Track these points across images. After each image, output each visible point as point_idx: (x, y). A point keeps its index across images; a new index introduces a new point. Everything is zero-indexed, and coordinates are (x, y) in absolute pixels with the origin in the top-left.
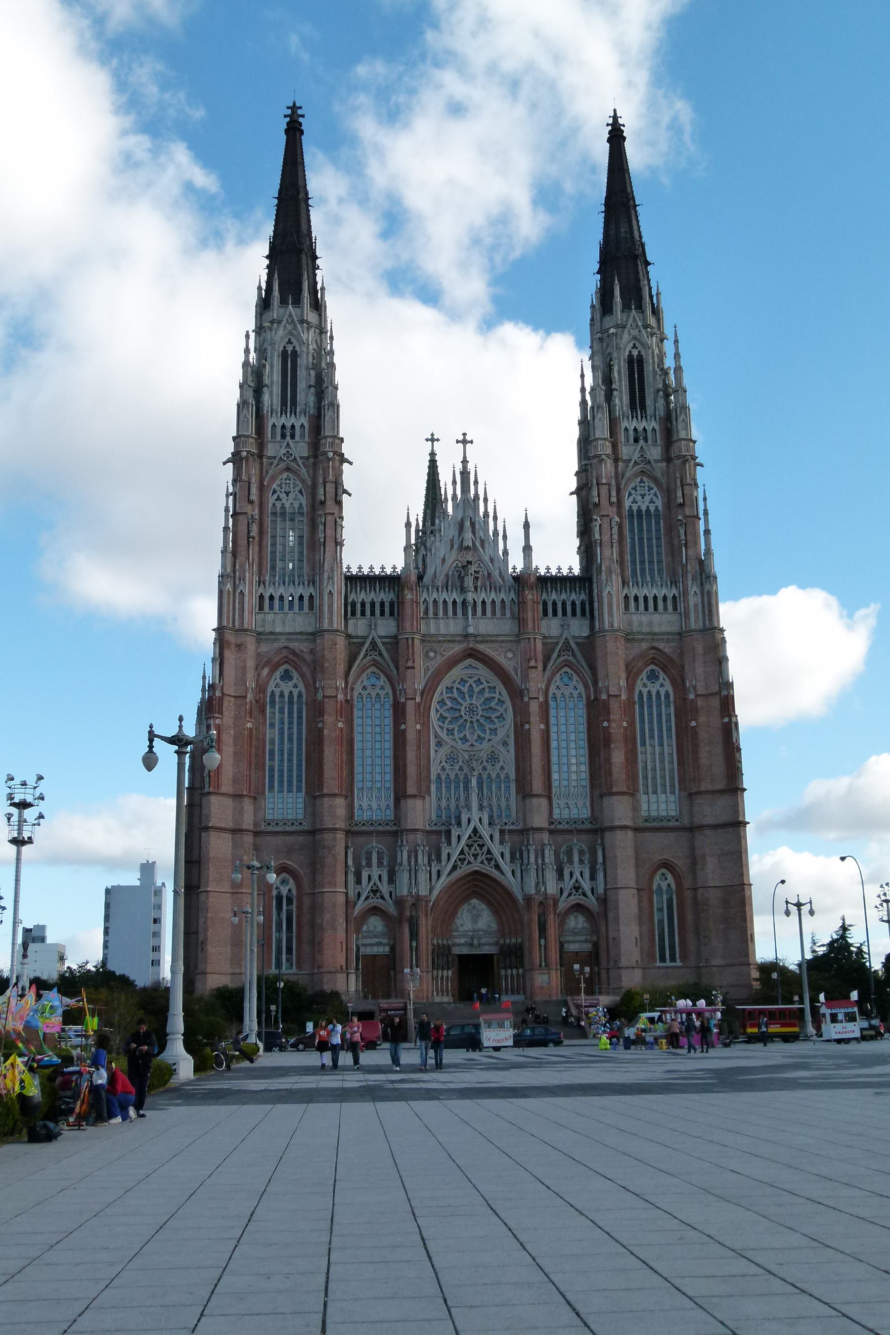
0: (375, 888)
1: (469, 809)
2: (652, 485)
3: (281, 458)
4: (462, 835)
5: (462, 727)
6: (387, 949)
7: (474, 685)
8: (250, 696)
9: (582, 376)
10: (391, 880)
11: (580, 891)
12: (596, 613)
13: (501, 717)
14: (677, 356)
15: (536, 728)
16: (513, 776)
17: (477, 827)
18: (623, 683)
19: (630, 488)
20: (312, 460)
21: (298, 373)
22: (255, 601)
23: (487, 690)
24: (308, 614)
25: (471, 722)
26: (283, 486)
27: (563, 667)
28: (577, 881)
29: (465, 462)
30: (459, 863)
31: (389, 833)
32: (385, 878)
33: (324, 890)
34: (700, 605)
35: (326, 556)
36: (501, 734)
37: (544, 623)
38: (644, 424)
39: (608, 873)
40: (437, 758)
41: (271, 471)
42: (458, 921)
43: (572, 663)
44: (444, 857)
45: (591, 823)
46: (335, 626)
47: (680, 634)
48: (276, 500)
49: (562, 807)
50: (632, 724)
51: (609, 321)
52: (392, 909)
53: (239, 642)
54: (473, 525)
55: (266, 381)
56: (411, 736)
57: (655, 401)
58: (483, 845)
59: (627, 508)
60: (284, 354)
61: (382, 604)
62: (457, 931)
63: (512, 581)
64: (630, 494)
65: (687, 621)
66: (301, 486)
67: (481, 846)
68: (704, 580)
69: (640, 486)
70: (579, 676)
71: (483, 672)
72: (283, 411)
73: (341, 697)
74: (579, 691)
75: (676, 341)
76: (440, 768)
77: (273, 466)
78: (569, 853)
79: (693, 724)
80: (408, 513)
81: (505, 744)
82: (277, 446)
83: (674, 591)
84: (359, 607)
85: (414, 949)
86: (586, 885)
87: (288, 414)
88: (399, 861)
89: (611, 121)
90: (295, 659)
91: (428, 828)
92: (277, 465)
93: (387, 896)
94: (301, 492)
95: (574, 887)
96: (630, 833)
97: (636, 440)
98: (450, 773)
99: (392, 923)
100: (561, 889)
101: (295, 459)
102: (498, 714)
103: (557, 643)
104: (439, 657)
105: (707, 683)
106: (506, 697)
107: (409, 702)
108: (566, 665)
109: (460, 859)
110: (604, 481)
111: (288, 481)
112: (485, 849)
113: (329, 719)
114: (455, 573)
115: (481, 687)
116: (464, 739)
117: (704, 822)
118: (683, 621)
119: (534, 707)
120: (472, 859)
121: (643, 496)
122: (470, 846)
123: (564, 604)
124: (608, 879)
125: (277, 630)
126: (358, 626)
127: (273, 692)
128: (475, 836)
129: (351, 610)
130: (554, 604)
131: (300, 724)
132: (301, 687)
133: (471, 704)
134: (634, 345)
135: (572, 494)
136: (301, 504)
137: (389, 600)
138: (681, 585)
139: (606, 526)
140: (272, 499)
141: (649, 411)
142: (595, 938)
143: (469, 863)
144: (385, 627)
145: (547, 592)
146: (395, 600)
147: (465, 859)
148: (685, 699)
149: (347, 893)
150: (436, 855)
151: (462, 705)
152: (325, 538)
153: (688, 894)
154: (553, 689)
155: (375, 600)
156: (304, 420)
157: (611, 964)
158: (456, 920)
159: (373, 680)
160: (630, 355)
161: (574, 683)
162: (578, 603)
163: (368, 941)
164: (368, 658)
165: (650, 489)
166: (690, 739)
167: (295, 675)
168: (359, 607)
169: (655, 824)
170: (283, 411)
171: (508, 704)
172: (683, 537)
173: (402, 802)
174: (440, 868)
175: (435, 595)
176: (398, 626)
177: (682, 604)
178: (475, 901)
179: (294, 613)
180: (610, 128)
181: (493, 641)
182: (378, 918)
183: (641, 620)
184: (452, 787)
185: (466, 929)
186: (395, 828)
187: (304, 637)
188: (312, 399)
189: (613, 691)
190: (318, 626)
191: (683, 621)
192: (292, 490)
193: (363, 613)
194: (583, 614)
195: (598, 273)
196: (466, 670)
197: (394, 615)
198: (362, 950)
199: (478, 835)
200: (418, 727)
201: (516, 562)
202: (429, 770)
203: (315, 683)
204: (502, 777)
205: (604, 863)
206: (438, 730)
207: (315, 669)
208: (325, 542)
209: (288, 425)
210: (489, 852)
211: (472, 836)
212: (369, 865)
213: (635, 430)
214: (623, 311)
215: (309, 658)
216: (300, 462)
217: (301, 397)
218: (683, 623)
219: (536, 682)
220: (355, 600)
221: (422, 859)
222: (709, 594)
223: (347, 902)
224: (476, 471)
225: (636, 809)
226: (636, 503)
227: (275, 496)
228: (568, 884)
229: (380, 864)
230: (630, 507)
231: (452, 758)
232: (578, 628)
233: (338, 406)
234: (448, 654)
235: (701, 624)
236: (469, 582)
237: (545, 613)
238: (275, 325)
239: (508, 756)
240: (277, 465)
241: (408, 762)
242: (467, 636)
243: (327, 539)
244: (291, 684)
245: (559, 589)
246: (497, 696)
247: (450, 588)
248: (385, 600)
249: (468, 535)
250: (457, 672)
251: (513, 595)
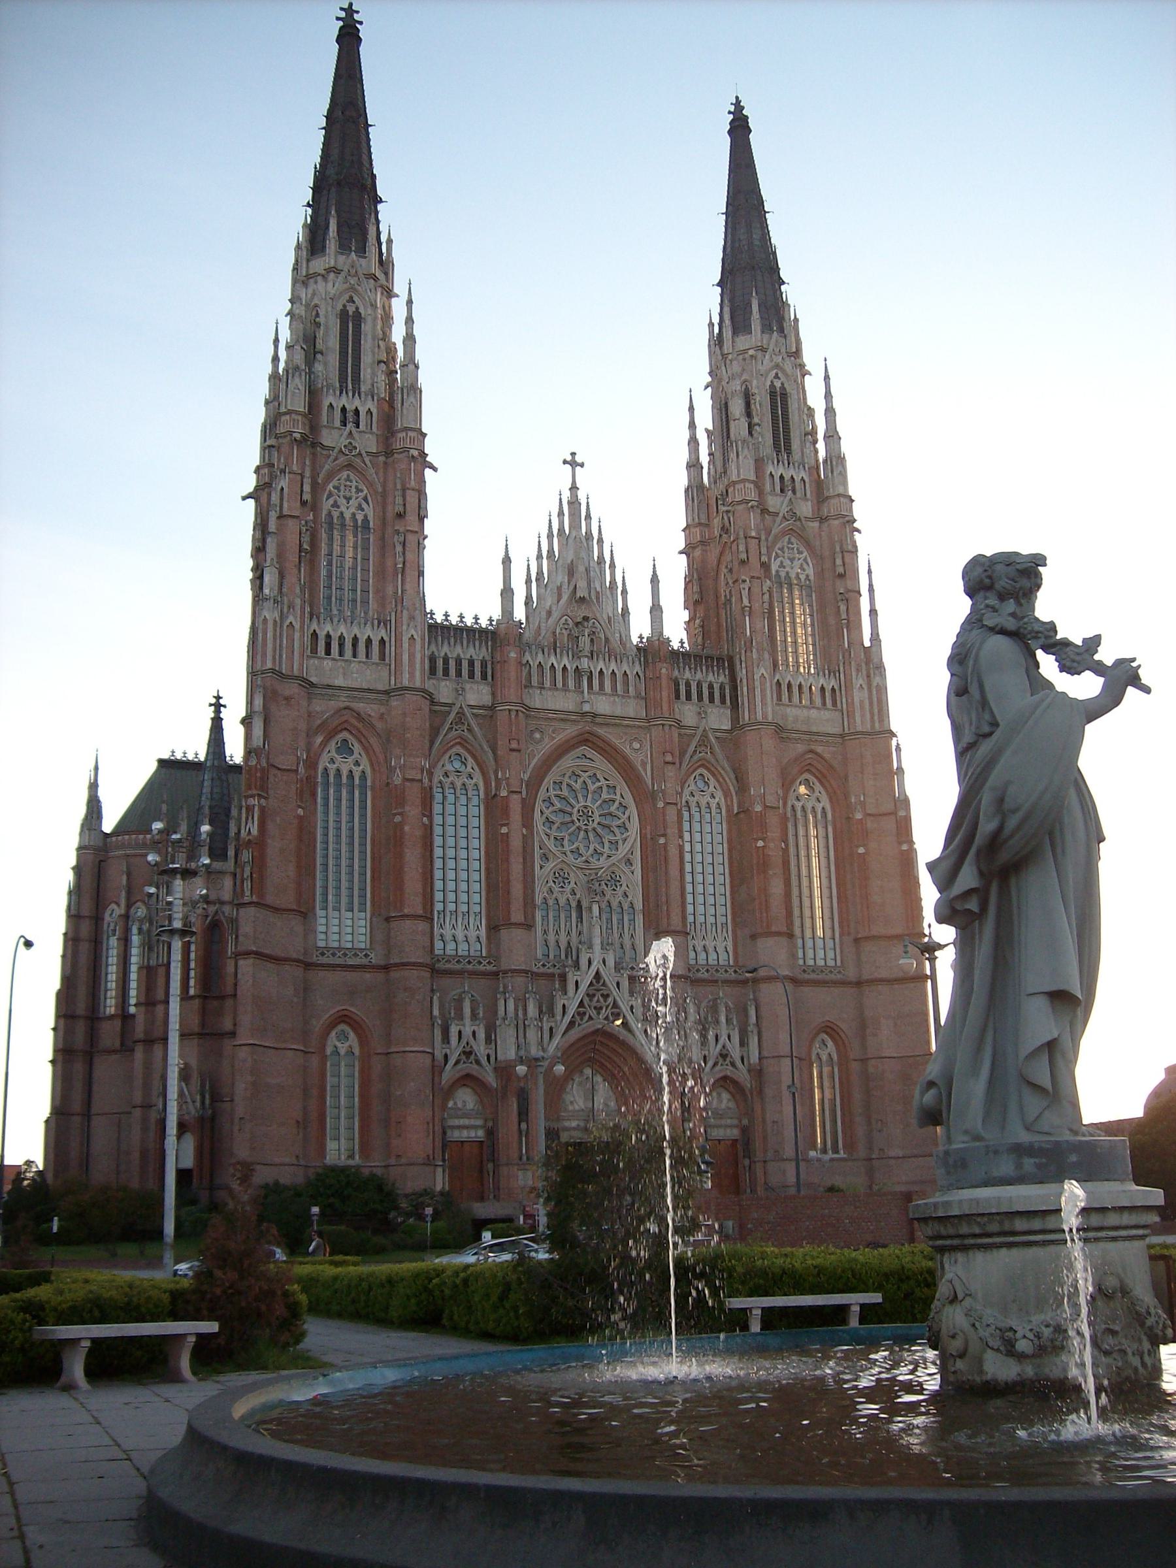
0: (468, 1049)
1: (590, 947)
2: (802, 549)
3: (341, 451)
4: (582, 980)
5: (574, 836)
6: (481, 1133)
7: (589, 782)
8: (301, 769)
9: (691, 409)
10: (488, 1040)
11: (728, 1059)
12: (743, 699)
13: (624, 827)
14: (828, 396)
16: (639, 905)
17: (601, 970)
18: (780, 792)
19: (776, 549)
20: (382, 459)
21: (362, 342)
22: (307, 639)
23: (605, 789)
24: (377, 664)
25: (586, 831)
26: (342, 488)
27: (699, 767)
28: (724, 1047)
29: (574, 488)
30: (578, 1018)
31: (484, 974)
32: (481, 1035)
33: (407, 1049)
34: (867, 702)
35: (407, 587)
36: (623, 850)
37: (677, 706)
38: (792, 472)
39: (764, 1038)
41: (327, 467)
42: (568, 1098)
43: (709, 762)
44: (558, 1010)
45: (735, 972)
46: (418, 684)
47: (842, 736)
48: (332, 506)
49: (699, 949)
50: (787, 845)
51: (743, 342)
52: (491, 1079)
53: (287, 693)
54: (587, 571)
55: (319, 346)
56: (516, 843)
57: (803, 443)
58: (608, 996)
59: (774, 572)
60: (344, 315)
61: (471, 663)
62: (566, 1110)
63: (635, 650)
64: (777, 556)
65: (852, 721)
66: (366, 491)
67: (606, 997)
68: (872, 672)
69: (788, 548)
70: (718, 781)
71: (601, 764)
72: (343, 389)
73: (426, 781)
74: (717, 800)
75: (827, 378)
76: (545, 890)
77: (332, 458)
78: (714, 1008)
79: (861, 850)
80: (507, 545)
81: (629, 862)
82: (335, 433)
83: (833, 683)
84: (440, 663)
85: (524, 1133)
86: (735, 1052)
87: (350, 394)
88: (501, 1012)
89: (732, 109)
90: (360, 726)
91: (535, 970)
92: (336, 459)
93: (484, 1061)
94: (365, 499)
95: (721, 1055)
96: (790, 987)
97: (782, 491)
98: (559, 896)
100: (705, 1057)
101: (360, 454)
102: (619, 822)
103: (693, 736)
104: (546, 740)
105: (877, 800)
106: (629, 800)
107: (515, 796)
108: (702, 766)
109: (579, 1014)
110: (753, 534)
111: (348, 483)
112: (610, 1000)
113: (413, 811)
114: (564, 631)
115: (598, 784)
116: (577, 852)
117: (877, 975)
118: (846, 719)
119: (671, 812)
120: (593, 1013)
121: (792, 560)
122: (591, 996)
123: (699, 685)
124: (764, 1045)
125: (337, 682)
127: (326, 769)
128: (598, 982)
130: (688, 685)
131: (363, 816)
132: (365, 764)
133: (586, 807)
134: (777, 374)
135: (681, 552)
136: (366, 516)
137: (481, 658)
138: (842, 676)
139: (756, 590)
140: (326, 505)
141: (796, 456)
142: (745, 1122)
143: (591, 1018)
144: (477, 694)
145: (679, 668)
146: (488, 658)
147: (584, 1013)
148: (848, 818)
149: (433, 1054)
150: (547, 1009)
151: (573, 807)
152: (404, 563)
153: (855, 1066)
154: (686, 795)
155: (462, 656)
156: (371, 405)
157: (770, 1154)
158: (564, 1096)
159: (457, 765)
160: (772, 385)
161: (712, 788)
162: (716, 687)
163: (456, 1122)
164: (453, 733)
165: (800, 553)
166: (856, 869)
167: (357, 748)
168: (440, 663)
169: (813, 976)
170: (343, 389)
171: (633, 810)
172: (844, 616)
173: (504, 933)
174: (553, 1025)
175: (540, 658)
176: (493, 694)
177: (844, 700)
178: (588, 1071)
179: (360, 662)
180: (731, 117)
181: (615, 725)
182: (468, 1090)
183: (795, 715)
184: (562, 916)
185: (577, 1107)
186: (489, 968)
187: (373, 696)
188: (382, 378)
189: (771, 800)
190: (393, 682)
191: (846, 719)
192: (354, 495)
193: (446, 672)
194: (723, 701)
195: (718, 285)
196: (577, 760)
197: (486, 679)
198: (449, 1133)
199: (602, 981)
200: (524, 831)
201: (639, 628)
202: (533, 891)
203: (387, 761)
204: (626, 906)
205: (758, 1024)
206: (543, 836)
207: (388, 741)
208: (403, 568)
209: (350, 408)
210: (615, 1005)
211: (594, 981)
212: (460, 1017)
213: (782, 477)
214: (763, 332)
215: (379, 725)
216: (367, 460)
217: (366, 373)
218: (846, 723)
220: (436, 654)
221: (532, 1010)
222: (882, 690)
223: (433, 1067)
224: (588, 503)
225: (794, 956)
226: (784, 567)
227: (331, 501)
228: (714, 1051)
229: (474, 1016)
230: (777, 571)
231: (561, 877)
232: (719, 719)
233: (421, 391)
234: (560, 737)
235: (869, 726)
236: (585, 642)
237: (678, 697)
238: (332, 275)
239: (634, 879)
240: (336, 459)
241: (511, 878)
242: (584, 714)
243: (407, 565)
244: (350, 760)
245: (693, 666)
246: (618, 797)
247: (558, 650)
248: (475, 657)
250: (568, 762)
251: (637, 668)
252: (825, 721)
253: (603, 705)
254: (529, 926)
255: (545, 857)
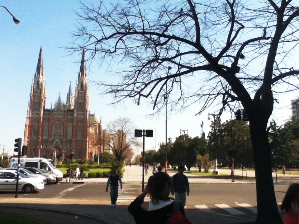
1: (56, 138)
15: (65, 129)
18: (76, 124)
40: (53, 132)
52: (46, 150)
71: (60, 122)
86: (70, 148)
99: (46, 151)
126: (45, 116)
129: (44, 114)
144: (48, 116)
183: (79, 116)
219: (65, 124)
228: (67, 148)
231: (55, 132)
232: (72, 117)
236: (59, 111)
249: (59, 105)
250: (56, 122)
252: (82, 116)
253: (60, 116)
254: (51, 137)
255: (54, 131)
